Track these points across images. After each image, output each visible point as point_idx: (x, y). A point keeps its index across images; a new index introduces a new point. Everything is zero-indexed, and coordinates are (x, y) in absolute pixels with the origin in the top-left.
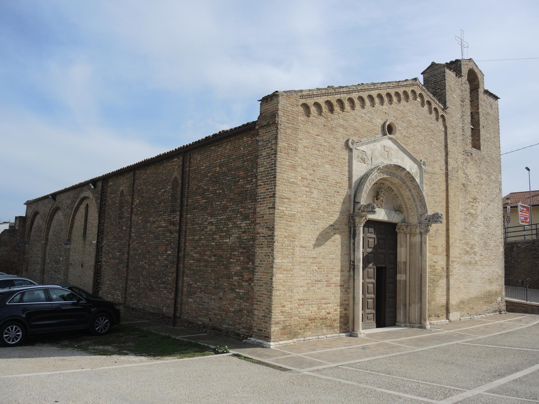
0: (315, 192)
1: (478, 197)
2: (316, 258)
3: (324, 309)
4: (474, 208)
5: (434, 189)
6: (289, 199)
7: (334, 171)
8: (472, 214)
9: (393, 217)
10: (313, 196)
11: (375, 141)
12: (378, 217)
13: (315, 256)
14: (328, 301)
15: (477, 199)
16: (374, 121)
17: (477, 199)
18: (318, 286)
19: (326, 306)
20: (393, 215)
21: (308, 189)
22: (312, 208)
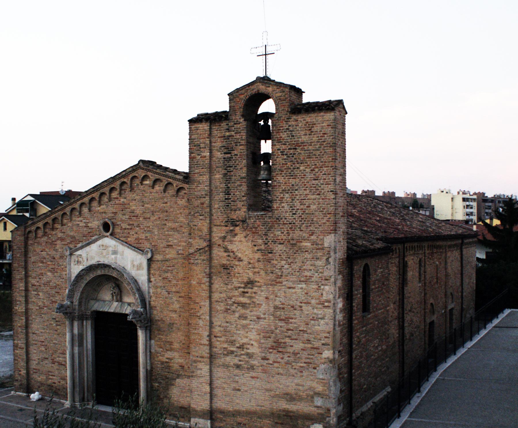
0: (41, 294)
1: (257, 279)
2: (43, 342)
3: (51, 379)
4: (247, 295)
5: (167, 279)
6: (20, 301)
7: (55, 276)
8: (242, 303)
9: (126, 309)
10: (40, 297)
11: (89, 244)
12: (108, 309)
13: (43, 340)
14: (54, 374)
15: (256, 282)
16: (89, 225)
17: (256, 282)
18: (46, 362)
19: (52, 377)
20: (126, 308)
21: (36, 293)
22: (40, 306)
